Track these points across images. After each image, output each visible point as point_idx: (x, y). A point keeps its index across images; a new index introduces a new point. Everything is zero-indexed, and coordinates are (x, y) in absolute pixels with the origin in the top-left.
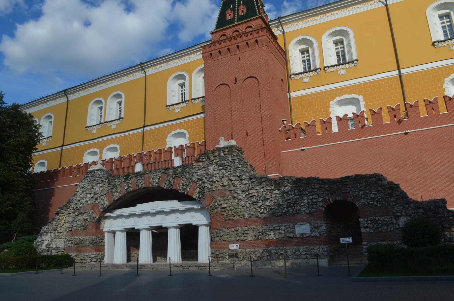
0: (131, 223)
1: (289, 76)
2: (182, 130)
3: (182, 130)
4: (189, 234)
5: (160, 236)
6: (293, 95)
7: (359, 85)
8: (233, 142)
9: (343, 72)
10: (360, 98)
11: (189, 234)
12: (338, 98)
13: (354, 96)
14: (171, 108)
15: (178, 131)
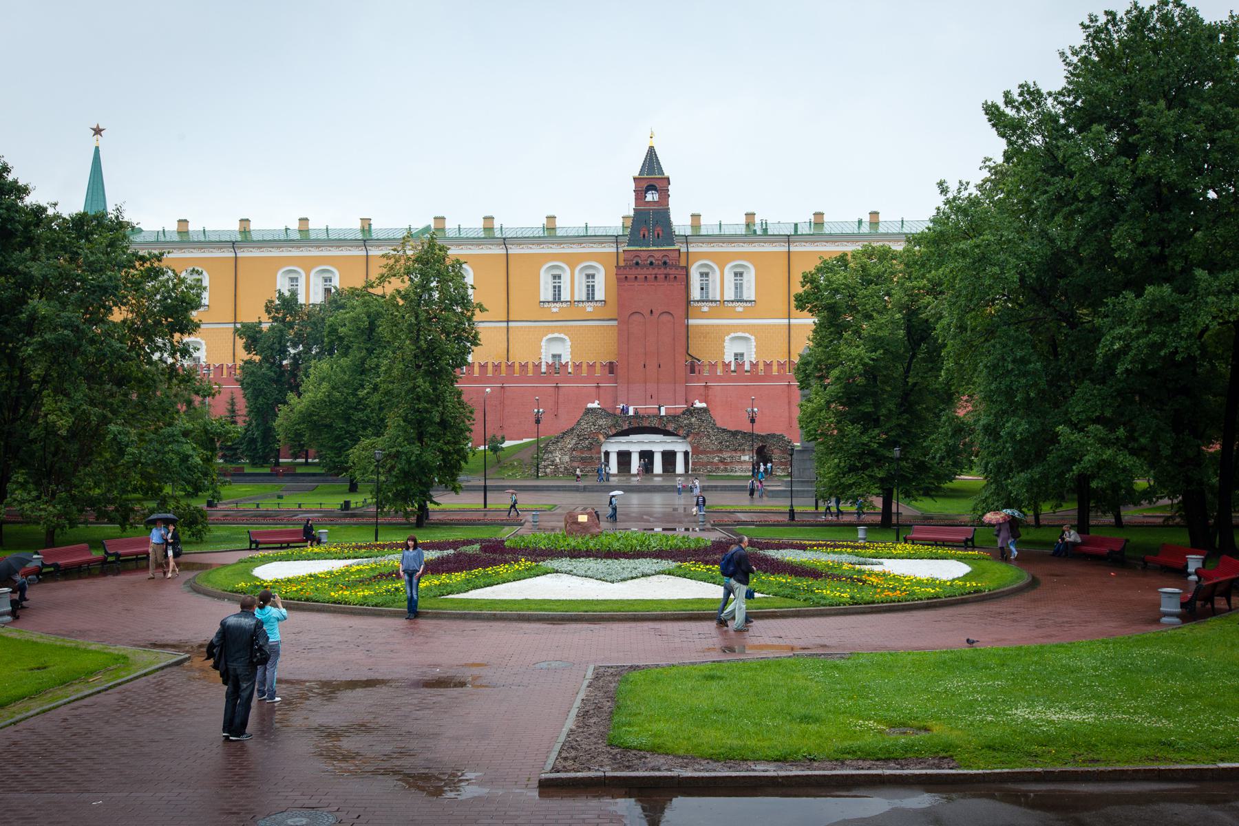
0: (624, 448)
1: (688, 302)
2: (562, 336)
3: (562, 336)
4: (669, 457)
5: (647, 456)
6: (691, 322)
7: (754, 326)
8: (704, 405)
9: (740, 309)
10: (753, 338)
11: (669, 457)
12: (733, 335)
13: (747, 335)
14: (546, 305)
15: (556, 335)
